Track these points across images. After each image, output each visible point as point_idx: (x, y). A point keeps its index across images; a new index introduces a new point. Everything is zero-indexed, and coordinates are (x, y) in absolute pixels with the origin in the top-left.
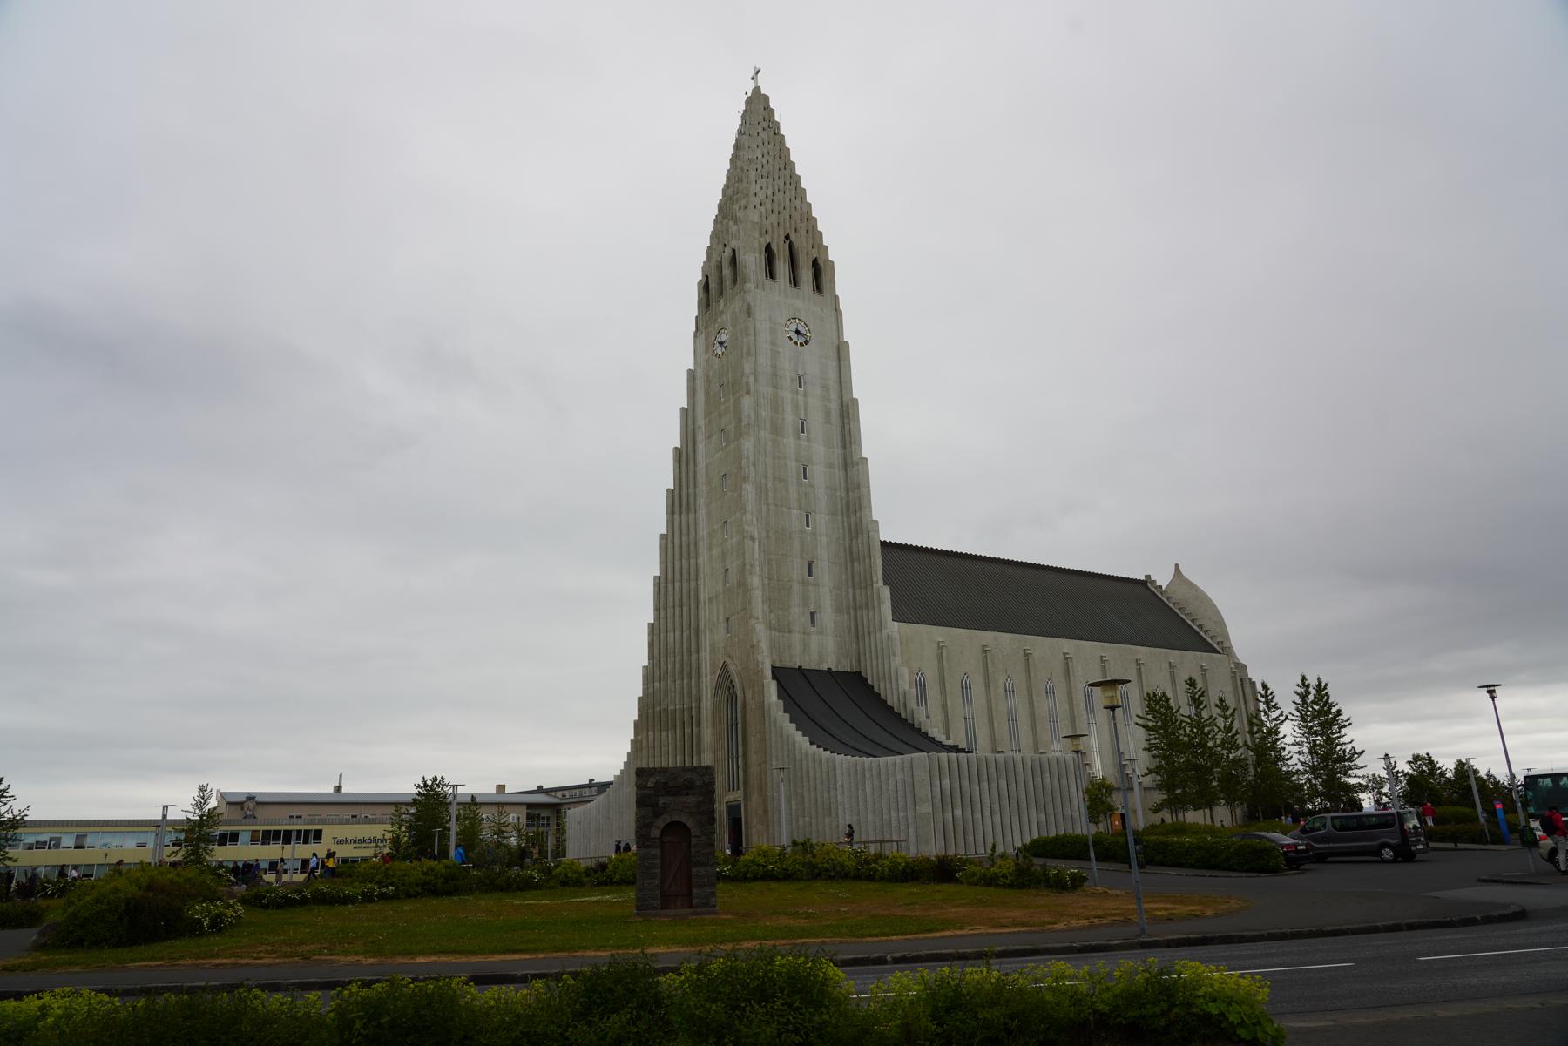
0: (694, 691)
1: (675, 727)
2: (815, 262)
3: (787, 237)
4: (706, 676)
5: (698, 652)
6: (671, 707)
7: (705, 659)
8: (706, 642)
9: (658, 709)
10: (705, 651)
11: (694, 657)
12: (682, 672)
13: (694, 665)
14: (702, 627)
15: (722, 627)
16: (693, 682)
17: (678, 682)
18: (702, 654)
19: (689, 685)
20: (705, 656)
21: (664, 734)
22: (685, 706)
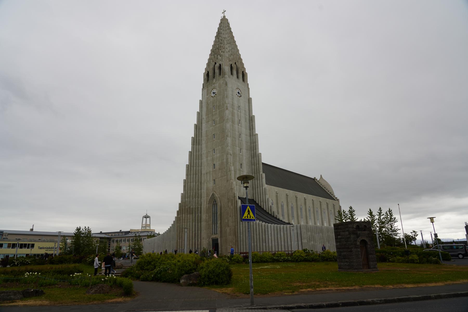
0: (199, 202)
1: (192, 213)
2: (220, 65)
4: (204, 198)
5: (201, 189)
6: (191, 207)
7: (204, 192)
8: (204, 187)
9: (187, 207)
10: (204, 190)
11: (200, 191)
12: (195, 196)
13: (200, 194)
14: (203, 182)
15: (212, 182)
16: (199, 199)
17: (194, 199)
18: (203, 191)
19: (198, 200)
20: (204, 191)
21: (189, 216)
22: (196, 207)
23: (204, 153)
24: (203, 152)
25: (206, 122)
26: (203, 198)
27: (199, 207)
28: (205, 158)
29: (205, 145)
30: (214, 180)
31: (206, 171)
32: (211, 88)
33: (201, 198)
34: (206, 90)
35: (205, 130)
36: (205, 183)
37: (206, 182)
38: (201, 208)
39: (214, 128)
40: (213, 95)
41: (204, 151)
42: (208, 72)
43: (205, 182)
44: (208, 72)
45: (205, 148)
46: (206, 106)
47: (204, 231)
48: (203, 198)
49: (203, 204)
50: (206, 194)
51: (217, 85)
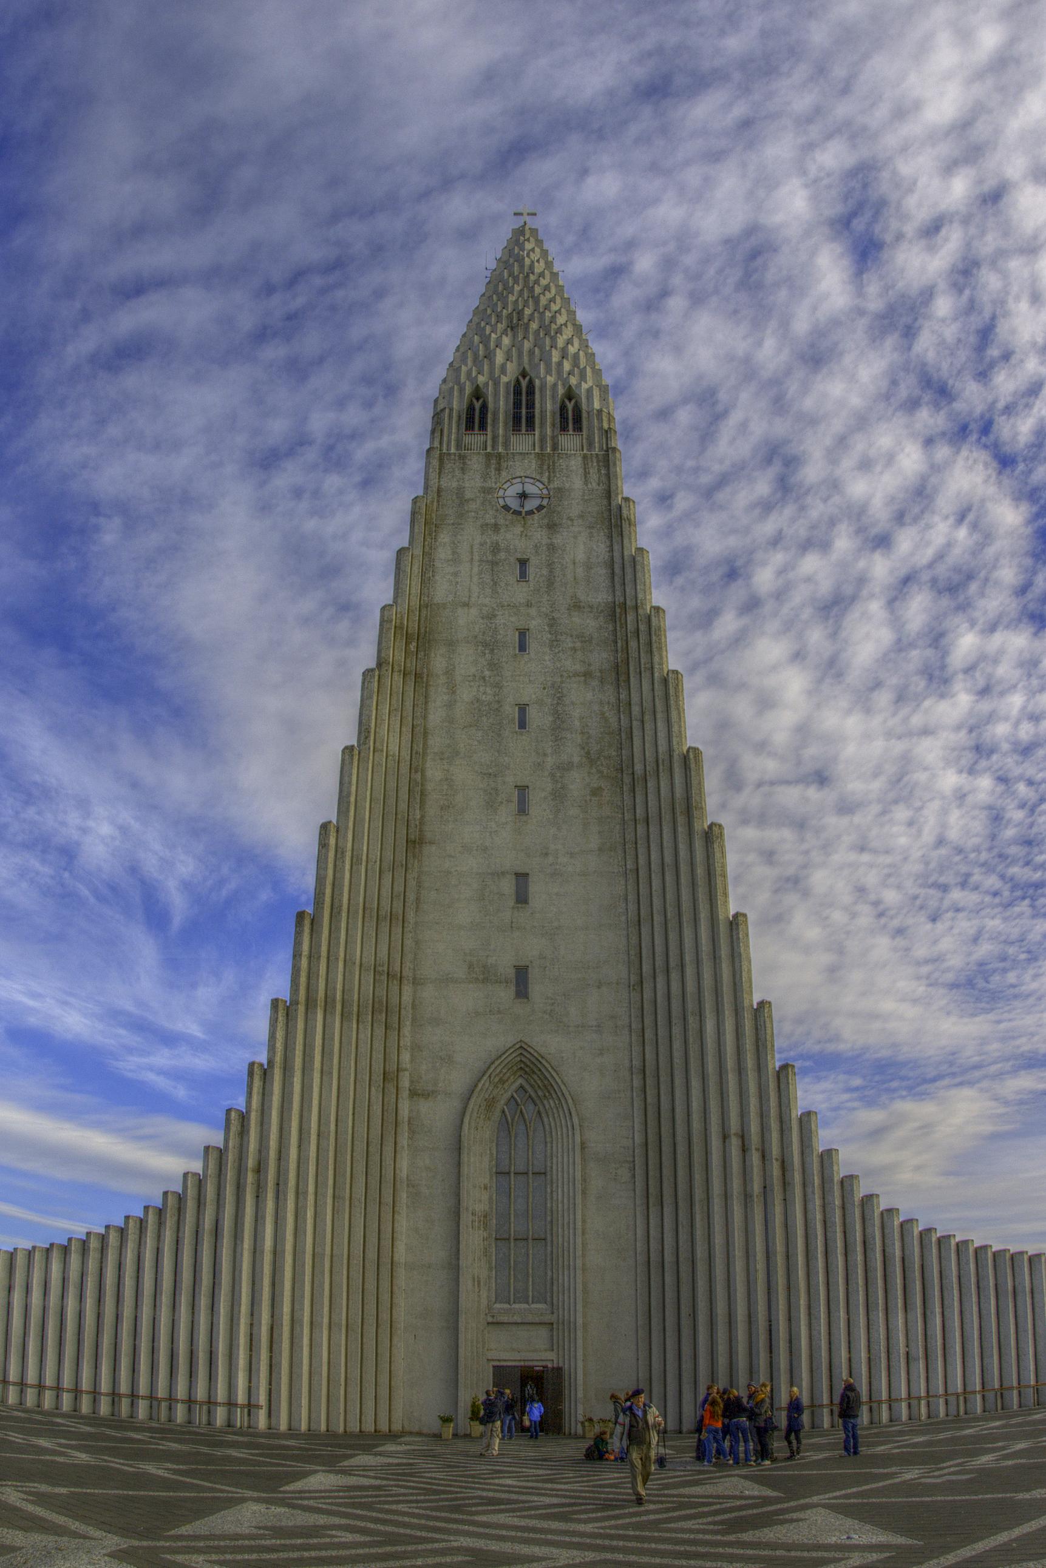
3: (524, 374)
42: (478, 394)
44: (478, 394)
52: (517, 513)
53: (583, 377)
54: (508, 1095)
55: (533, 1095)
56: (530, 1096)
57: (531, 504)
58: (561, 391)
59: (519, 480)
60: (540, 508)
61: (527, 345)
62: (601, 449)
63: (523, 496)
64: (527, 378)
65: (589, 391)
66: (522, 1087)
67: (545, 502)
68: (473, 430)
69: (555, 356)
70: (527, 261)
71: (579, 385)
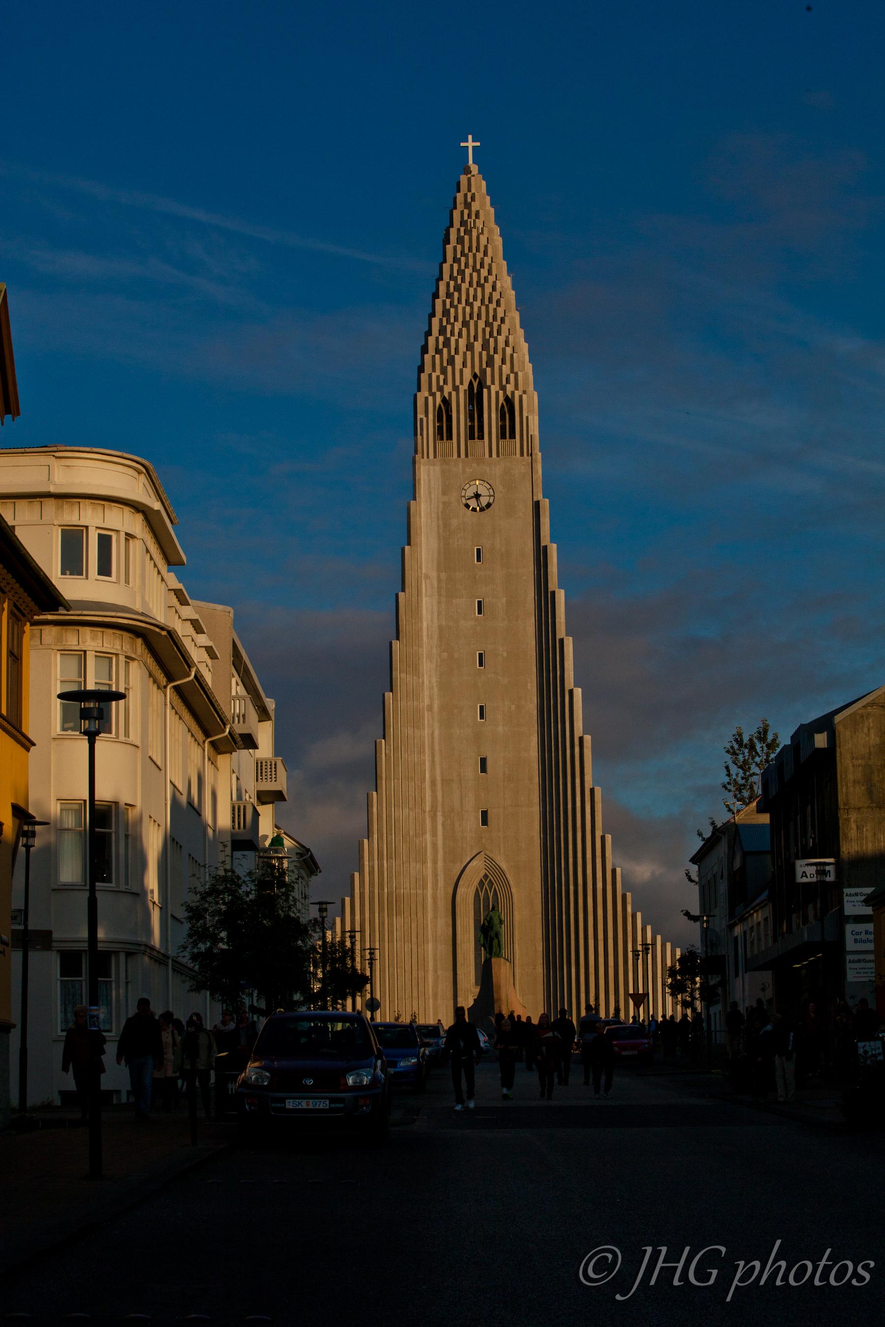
3: (475, 376)
4: (435, 862)
7: (434, 845)
10: (434, 834)
18: (428, 837)
23: (430, 708)
24: (427, 701)
25: (440, 595)
26: (429, 865)
27: (420, 891)
28: (436, 725)
29: (434, 680)
30: (485, 814)
31: (442, 774)
32: (464, 472)
33: (424, 862)
34: (438, 468)
35: (432, 621)
36: (439, 814)
37: (444, 812)
38: (424, 897)
39: (478, 629)
40: (473, 503)
41: (431, 697)
42: (446, 402)
43: (440, 808)
44: (446, 402)
45: (436, 690)
46: (439, 533)
47: (435, 971)
48: (429, 865)
49: (430, 885)
50: (445, 853)
51: (496, 468)
52: (474, 510)
53: (517, 388)
54: (478, 880)
55: (492, 879)
56: (490, 880)
57: (484, 501)
58: (501, 399)
59: (474, 482)
60: (489, 505)
61: (478, 346)
62: (528, 455)
63: (477, 496)
64: (478, 380)
65: (521, 397)
66: (486, 874)
67: (491, 501)
68: (442, 439)
69: (497, 358)
70: (474, 233)
71: (513, 393)
